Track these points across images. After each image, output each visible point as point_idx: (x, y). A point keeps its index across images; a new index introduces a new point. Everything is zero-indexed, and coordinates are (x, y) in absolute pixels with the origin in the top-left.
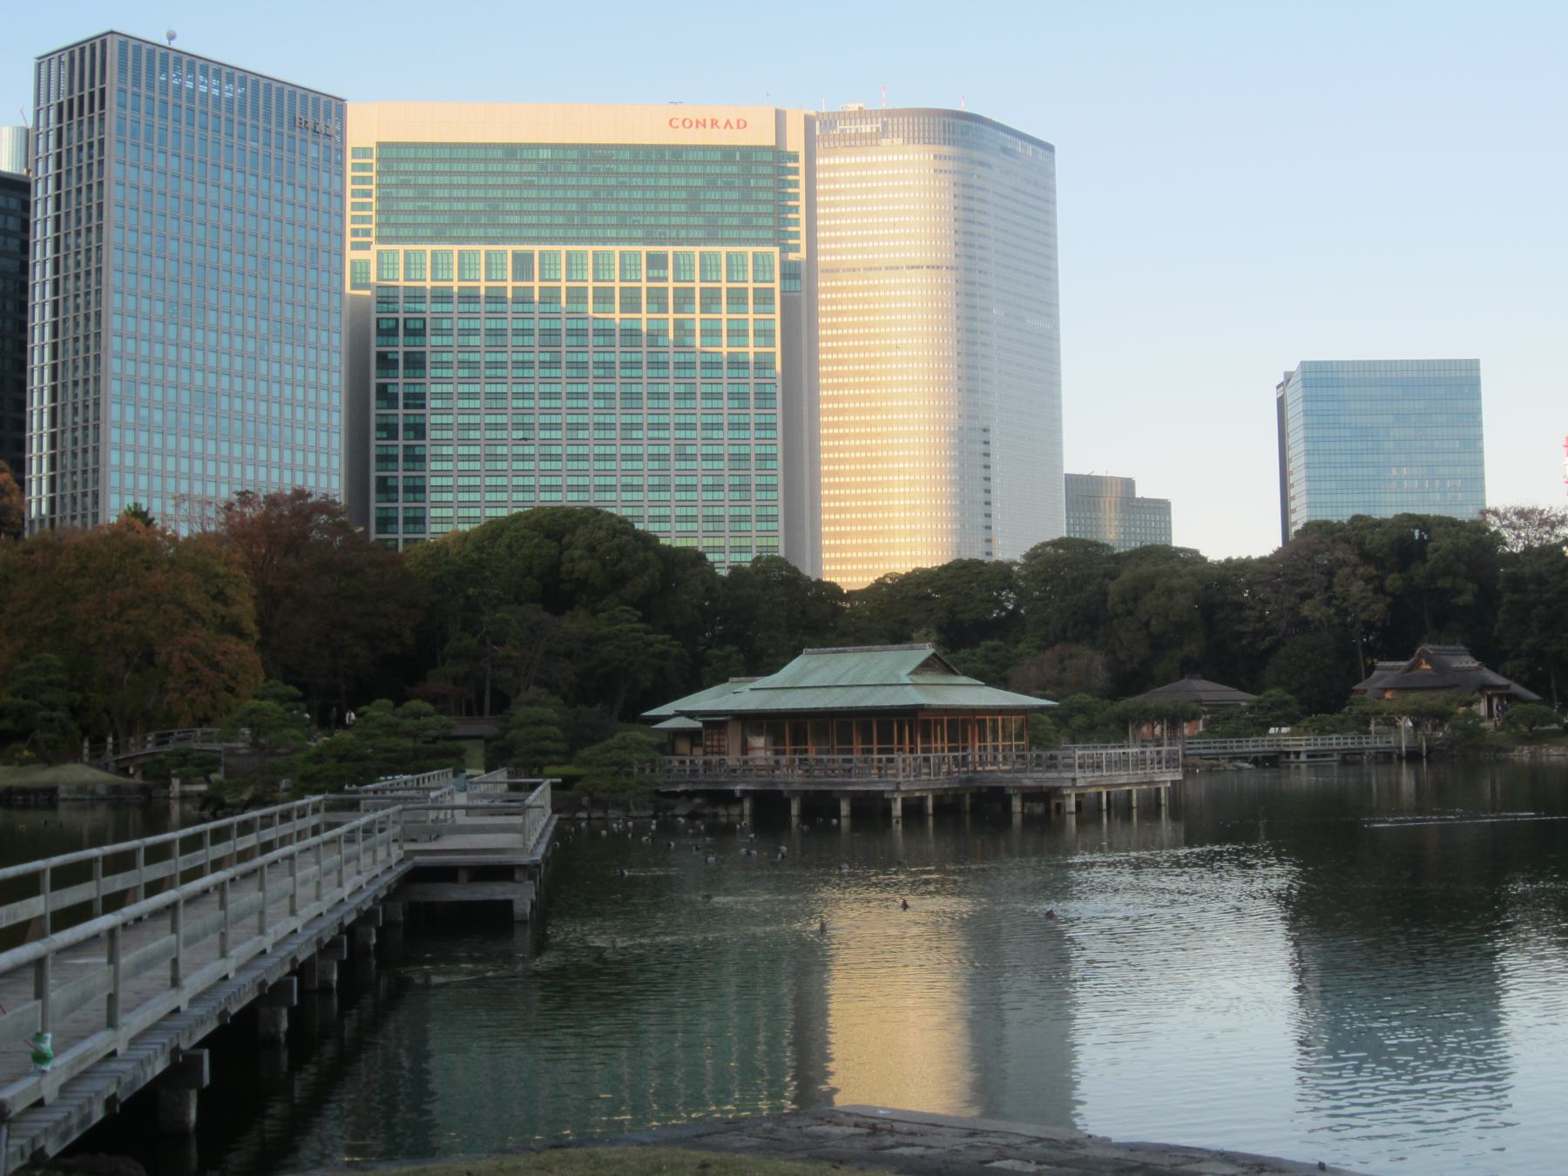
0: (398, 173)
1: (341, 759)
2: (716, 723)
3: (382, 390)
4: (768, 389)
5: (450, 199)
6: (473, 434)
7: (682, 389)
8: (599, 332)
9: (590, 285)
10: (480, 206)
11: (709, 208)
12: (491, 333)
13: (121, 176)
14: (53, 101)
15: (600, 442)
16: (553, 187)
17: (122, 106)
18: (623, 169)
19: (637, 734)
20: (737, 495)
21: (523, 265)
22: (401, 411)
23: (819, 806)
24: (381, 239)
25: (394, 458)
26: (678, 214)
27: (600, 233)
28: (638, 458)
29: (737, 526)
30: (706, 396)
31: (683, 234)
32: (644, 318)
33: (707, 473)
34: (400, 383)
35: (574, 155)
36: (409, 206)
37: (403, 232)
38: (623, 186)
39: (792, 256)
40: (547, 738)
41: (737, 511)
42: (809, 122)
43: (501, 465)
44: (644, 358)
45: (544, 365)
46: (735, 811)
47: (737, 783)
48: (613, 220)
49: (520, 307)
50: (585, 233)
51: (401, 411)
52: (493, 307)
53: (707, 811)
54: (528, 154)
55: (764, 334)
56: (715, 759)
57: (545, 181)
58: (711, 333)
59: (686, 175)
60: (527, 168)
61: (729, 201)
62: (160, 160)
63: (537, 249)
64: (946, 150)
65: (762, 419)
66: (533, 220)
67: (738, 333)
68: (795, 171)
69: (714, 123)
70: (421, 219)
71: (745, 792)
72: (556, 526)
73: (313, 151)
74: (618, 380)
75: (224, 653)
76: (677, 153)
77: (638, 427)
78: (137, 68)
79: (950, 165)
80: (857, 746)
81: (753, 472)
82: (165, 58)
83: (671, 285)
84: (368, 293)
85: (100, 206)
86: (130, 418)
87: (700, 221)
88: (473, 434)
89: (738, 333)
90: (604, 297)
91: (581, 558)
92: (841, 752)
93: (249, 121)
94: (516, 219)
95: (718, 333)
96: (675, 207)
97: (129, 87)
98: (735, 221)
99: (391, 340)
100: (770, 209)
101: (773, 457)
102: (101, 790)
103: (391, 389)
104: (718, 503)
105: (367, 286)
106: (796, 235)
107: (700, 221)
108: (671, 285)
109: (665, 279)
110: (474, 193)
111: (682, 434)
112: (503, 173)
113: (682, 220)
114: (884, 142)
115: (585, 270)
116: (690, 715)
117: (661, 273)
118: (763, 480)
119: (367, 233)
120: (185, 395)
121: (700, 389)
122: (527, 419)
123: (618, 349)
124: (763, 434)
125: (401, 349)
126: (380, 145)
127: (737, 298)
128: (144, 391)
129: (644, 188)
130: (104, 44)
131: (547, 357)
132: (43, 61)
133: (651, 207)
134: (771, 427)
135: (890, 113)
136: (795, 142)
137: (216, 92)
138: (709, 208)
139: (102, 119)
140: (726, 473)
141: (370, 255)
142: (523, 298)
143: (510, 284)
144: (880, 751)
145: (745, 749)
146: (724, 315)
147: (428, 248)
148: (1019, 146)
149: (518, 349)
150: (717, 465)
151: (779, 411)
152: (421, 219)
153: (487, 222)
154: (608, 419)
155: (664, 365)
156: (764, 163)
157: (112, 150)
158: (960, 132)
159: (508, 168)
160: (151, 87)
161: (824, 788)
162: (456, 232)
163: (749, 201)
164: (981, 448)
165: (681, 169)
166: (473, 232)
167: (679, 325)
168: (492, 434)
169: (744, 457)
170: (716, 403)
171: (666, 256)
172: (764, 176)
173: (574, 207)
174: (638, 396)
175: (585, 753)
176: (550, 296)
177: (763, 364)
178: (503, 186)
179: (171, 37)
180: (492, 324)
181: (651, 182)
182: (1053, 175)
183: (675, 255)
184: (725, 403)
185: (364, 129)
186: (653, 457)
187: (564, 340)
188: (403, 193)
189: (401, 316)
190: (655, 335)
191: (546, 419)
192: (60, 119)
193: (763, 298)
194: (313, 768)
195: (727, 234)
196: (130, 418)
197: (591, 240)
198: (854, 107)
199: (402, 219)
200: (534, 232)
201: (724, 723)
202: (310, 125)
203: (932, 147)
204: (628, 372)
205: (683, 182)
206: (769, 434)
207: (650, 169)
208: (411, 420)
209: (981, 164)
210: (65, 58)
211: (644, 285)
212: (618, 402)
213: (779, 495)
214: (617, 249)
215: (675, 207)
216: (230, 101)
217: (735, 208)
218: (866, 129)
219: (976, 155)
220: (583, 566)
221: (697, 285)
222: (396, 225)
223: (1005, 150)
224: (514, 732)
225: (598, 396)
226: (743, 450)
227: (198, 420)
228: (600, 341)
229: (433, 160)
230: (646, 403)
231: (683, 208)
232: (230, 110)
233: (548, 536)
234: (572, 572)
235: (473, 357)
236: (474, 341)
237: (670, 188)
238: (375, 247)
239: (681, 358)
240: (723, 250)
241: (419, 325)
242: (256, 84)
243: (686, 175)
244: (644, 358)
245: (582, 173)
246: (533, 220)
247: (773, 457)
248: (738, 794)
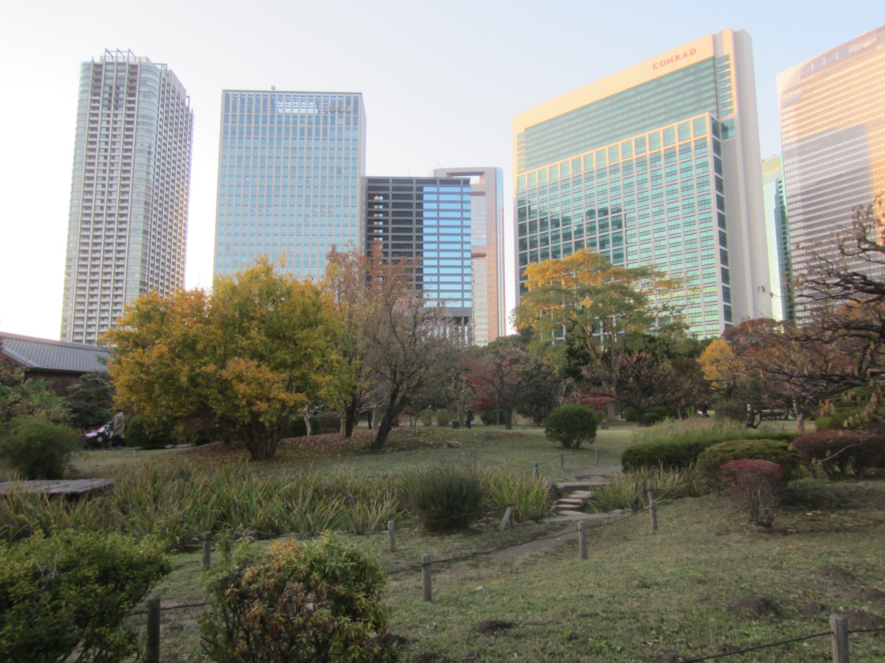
4: (706, 197)
21: (576, 163)
39: (730, 116)
63: (581, 155)
65: (703, 216)
101: (710, 238)
109: (645, 151)
114: (879, 47)
117: (643, 149)
126: (526, 130)
155: (645, 199)
171: (644, 139)
193: (701, 145)
218: (866, 44)
247: (710, 238)
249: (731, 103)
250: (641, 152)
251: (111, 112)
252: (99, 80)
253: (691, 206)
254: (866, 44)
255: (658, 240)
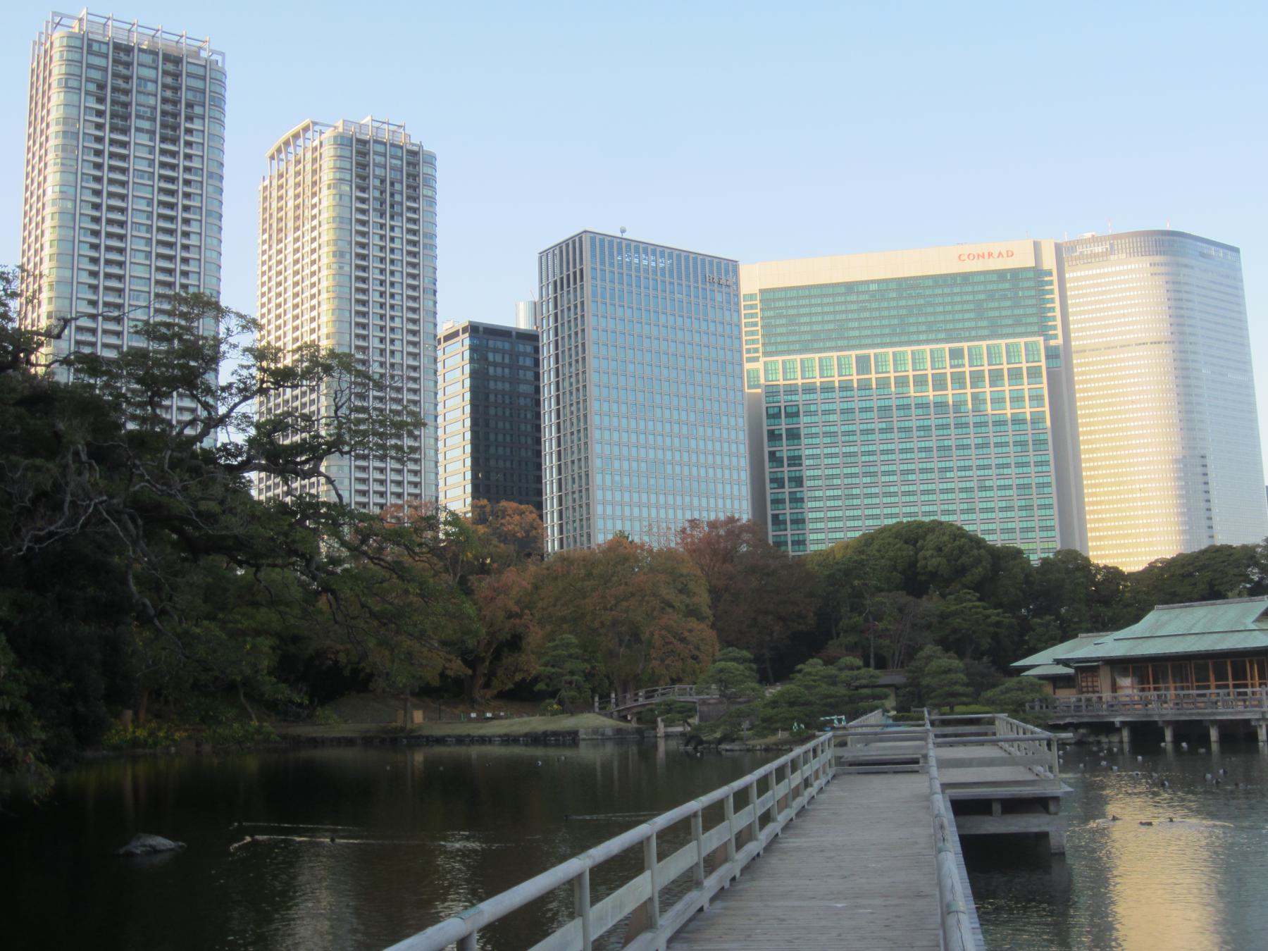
0: (775, 308)
1: (791, 704)
2: (1088, 668)
3: (772, 454)
4: (1042, 437)
5: (811, 323)
6: (836, 482)
7: (980, 441)
8: (919, 406)
9: (911, 374)
10: (831, 326)
11: (991, 314)
12: (843, 412)
13: (595, 323)
14: (551, 280)
15: (923, 482)
16: (880, 309)
17: (594, 278)
18: (928, 292)
19: (1011, 682)
20: (1024, 513)
21: (863, 364)
22: (786, 469)
23: (1191, 733)
24: (765, 354)
25: (783, 501)
26: (969, 320)
27: (915, 337)
28: (951, 491)
29: (1025, 535)
30: (998, 445)
31: (973, 333)
32: (950, 394)
33: (1002, 498)
34: (784, 450)
35: (894, 285)
36: (783, 330)
37: (780, 348)
38: (930, 304)
39: (1052, 343)
40: (956, 683)
41: (1025, 525)
42: (1058, 248)
43: (856, 502)
44: (951, 421)
45: (882, 431)
46: (1115, 739)
47: (1115, 716)
48: (923, 328)
49: (863, 393)
50: (904, 338)
51: (786, 469)
52: (844, 394)
53: (1091, 739)
54: (862, 288)
55: (1036, 398)
56: (1094, 696)
57: (875, 305)
58: (998, 401)
59: (974, 293)
60: (862, 298)
61: (1004, 308)
62: (620, 312)
63: (872, 352)
64: (1158, 259)
65: (1039, 459)
66: (868, 332)
67: (1017, 399)
68: (1051, 283)
69: (990, 255)
70: (792, 338)
71: (1123, 723)
72: (913, 535)
73: (719, 297)
74: (934, 438)
75: (690, 631)
76: (966, 278)
77: (951, 469)
78: (602, 252)
79: (1162, 269)
80: (1213, 683)
81: (1035, 496)
82: (620, 244)
83: (967, 369)
84: (759, 391)
85: (583, 344)
86: (608, 483)
87: (985, 323)
88: (836, 482)
89: (1017, 399)
90: (920, 381)
91: (932, 556)
92: (1198, 688)
93: (676, 281)
94: (856, 333)
95: (1003, 400)
96: (967, 316)
97: (598, 267)
98: (1010, 322)
99: (777, 421)
100: (1034, 310)
101: (1048, 485)
102: (609, 732)
103: (778, 454)
104: (1011, 520)
105: (758, 386)
106: (1055, 328)
107: (985, 323)
108: (967, 369)
110: (827, 318)
111: (981, 472)
112: (845, 303)
113: (973, 324)
114: (1112, 257)
115: (907, 364)
116: (1066, 663)
118: (1042, 502)
119: (756, 351)
120: (643, 465)
121: (993, 440)
122: (872, 469)
123: (933, 416)
124: (1040, 469)
125: (784, 427)
126: (761, 291)
127: (1015, 375)
128: (617, 464)
129: (944, 304)
130: (580, 239)
131: (884, 425)
132: (543, 255)
133: (949, 317)
134: (1046, 463)
135: (1115, 237)
136: (1049, 262)
137: (653, 264)
138: (991, 314)
139: (582, 288)
140: (1015, 498)
141: (759, 365)
142: (865, 386)
143: (855, 378)
144: (1218, 687)
145: (1114, 688)
146: (1006, 388)
147: (798, 357)
148: (1213, 251)
149: (863, 421)
150: (1008, 493)
151: (1051, 452)
152: (792, 338)
153: (837, 337)
154: (929, 466)
155: (966, 425)
156: (1028, 279)
157: (590, 307)
158: (1168, 244)
159: (848, 298)
160: (612, 265)
161: (1194, 718)
162: (816, 345)
163: (1019, 307)
164: (1200, 470)
165: (970, 289)
166: (828, 344)
167: (975, 397)
168: (849, 481)
169: (1028, 486)
170: (1004, 450)
171: (962, 350)
172: (1029, 288)
173: (896, 321)
174: (949, 448)
175: (989, 694)
176: (883, 383)
177: (1037, 419)
178: (846, 312)
179: (623, 231)
180: (845, 406)
181: (949, 299)
182: (1240, 269)
183: (969, 348)
184: (1011, 449)
185: (751, 281)
186: (962, 490)
187: (895, 413)
188: (778, 322)
189: (782, 405)
190: (958, 405)
191: (886, 468)
192: (555, 291)
193: (1034, 373)
194: (770, 712)
195: (1004, 331)
196: (608, 483)
197: (909, 343)
198: (1088, 235)
199: (779, 340)
200: (869, 341)
201: (1097, 667)
202: (716, 280)
203: (1148, 258)
204: (941, 432)
205: (971, 298)
206: (1044, 469)
207: (947, 290)
208: (793, 474)
209: (1186, 266)
210: (557, 252)
211: (948, 371)
212: (935, 454)
213: (1054, 512)
214: (927, 348)
215: (967, 316)
216: (663, 269)
217: (1009, 312)
218: (1099, 249)
219: (1182, 260)
220: (933, 563)
221: (986, 368)
222: (776, 344)
223: (1203, 255)
224: (928, 679)
225: (921, 450)
226: (1026, 481)
227: (652, 481)
228: (920, 411)
229: (798, 298)
230: (955, 453)
231: (972, 315)
232: (663, 274)
233: (906, 542)
234: (926, 566)
235: (832, 429)
236: (832, 418)
237: (962, 302)
238: (762, 360)
239: (978, 420)
240: (1002, 342)
241: (795, 409)
242: (679, 256)
243: (974, 293)
244: (951, 421)
245: (900, 298)
246: (868, 332)
247: (1048, 485)
248: (1118, 725)
249: (1055, 328)
250: (959, 366)
251: (389, 223)
252: (363, 166)
253: (1023, 444)
254: (1099, 249)
255: (981, 479)
